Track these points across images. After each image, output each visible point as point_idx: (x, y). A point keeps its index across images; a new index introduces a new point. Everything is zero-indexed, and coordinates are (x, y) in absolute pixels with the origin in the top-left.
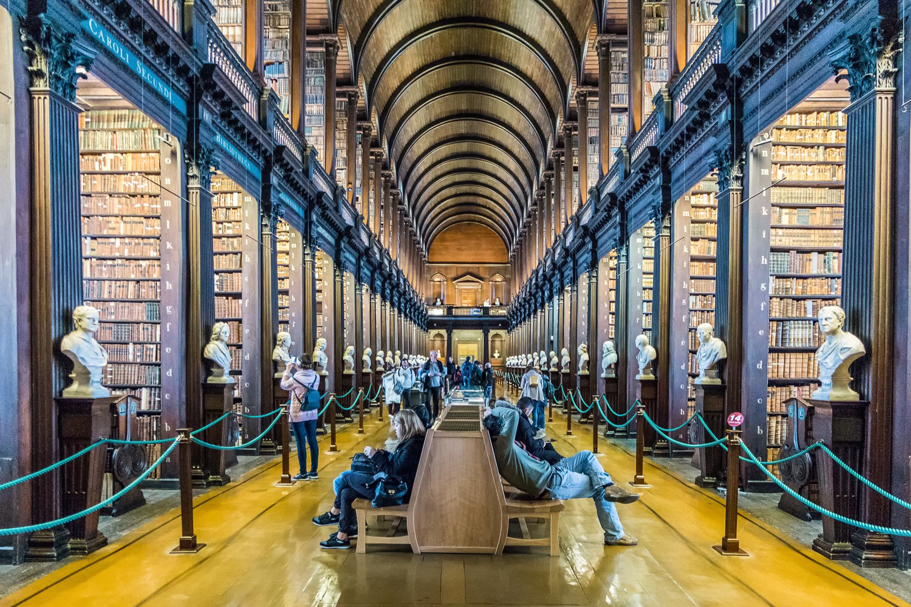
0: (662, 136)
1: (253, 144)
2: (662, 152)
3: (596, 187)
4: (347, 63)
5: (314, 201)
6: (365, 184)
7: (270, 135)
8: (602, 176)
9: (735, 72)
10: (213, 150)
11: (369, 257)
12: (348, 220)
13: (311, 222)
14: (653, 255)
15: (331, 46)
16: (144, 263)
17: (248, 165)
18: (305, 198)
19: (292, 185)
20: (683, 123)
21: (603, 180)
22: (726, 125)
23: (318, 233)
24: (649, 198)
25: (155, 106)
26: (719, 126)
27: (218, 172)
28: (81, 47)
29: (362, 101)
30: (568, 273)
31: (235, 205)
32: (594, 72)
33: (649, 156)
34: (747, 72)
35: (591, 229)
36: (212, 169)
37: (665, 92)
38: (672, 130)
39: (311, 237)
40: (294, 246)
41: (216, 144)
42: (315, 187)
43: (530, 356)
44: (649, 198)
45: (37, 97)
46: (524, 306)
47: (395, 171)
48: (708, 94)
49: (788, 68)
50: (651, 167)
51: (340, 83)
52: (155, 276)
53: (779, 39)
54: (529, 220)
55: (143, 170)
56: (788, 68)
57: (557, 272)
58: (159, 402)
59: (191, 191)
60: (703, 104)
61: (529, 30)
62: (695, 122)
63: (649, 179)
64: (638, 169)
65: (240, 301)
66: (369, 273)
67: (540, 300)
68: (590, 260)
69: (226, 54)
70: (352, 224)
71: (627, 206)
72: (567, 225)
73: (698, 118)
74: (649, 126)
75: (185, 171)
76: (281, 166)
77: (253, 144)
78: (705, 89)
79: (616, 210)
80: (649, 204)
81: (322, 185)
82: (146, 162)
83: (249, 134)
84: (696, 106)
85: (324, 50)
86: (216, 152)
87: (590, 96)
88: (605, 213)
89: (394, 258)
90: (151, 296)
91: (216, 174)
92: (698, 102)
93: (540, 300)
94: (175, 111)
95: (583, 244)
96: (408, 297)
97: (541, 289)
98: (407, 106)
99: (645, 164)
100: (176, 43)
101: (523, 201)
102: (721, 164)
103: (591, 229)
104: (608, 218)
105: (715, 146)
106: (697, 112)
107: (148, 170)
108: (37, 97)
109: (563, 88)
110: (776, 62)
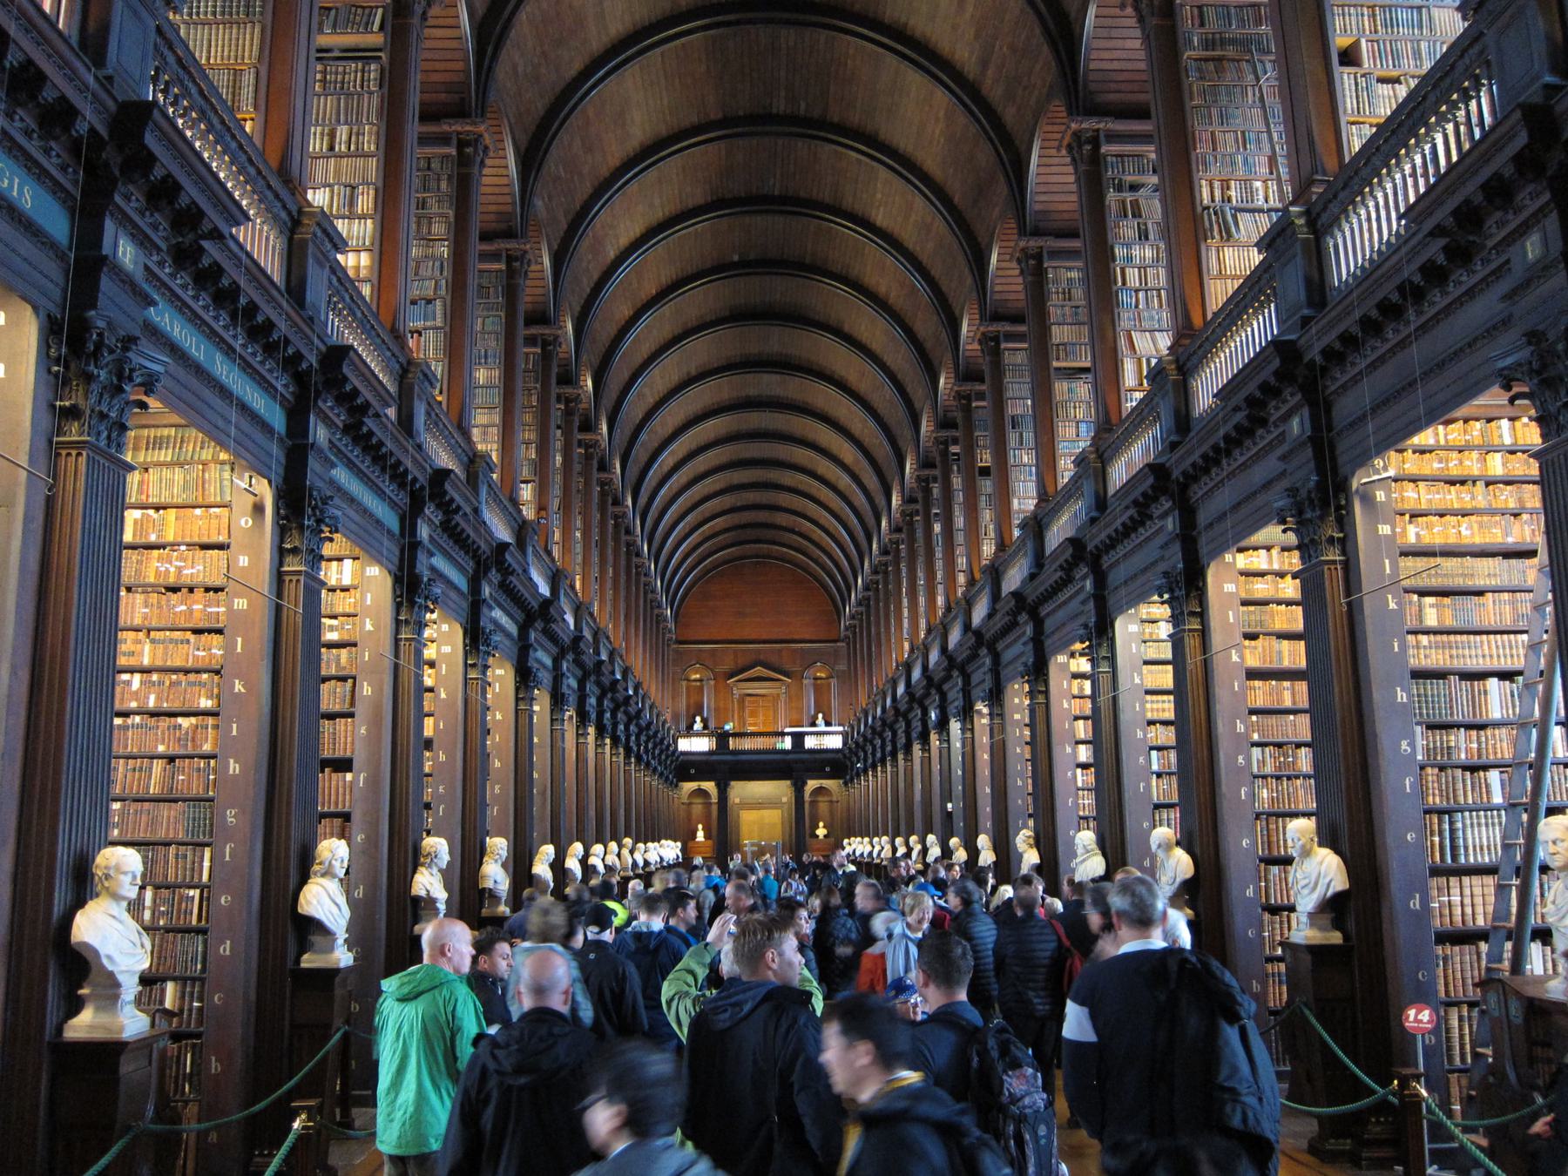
6: (566, 506)
10: (331, 498)
15: (468, 144)
18: (402, 485)
31: (347, 581)
45: (64, 452)
51: (531, 320)
55: (196, 539)
59: (287, 578)
75: (277, 539)
82: (203, 525)
86: (337, 501)
107: (205, 540)
108: (64, 452)
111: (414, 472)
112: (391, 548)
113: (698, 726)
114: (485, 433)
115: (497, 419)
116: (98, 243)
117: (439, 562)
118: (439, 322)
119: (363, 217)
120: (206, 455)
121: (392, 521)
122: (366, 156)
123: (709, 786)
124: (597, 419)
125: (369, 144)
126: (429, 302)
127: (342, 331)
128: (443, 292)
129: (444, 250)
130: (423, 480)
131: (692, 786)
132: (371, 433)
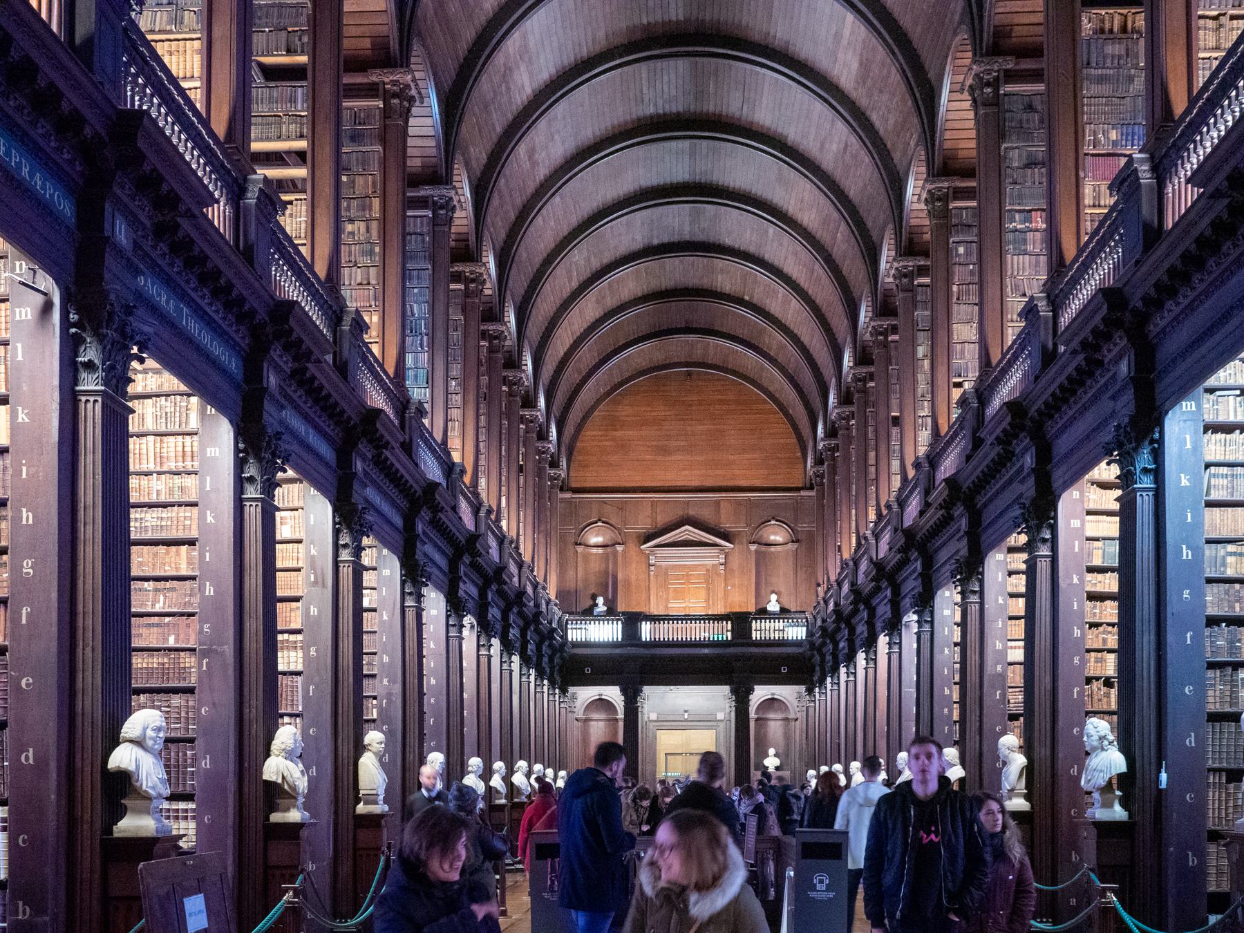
3: (928, 456)
4: (429, 121)
7: (417, 465)
8: (1057, 265)
9: (1136, 303)
11: (475, 554)
14: (1023, 590)
17: (218, 350)
19: (309, 392)
21: (990, 376)
22: (1127, 383)
29: (463, 218)
30: (912, 585)
32: (962, 145)
33: (1009, 418)
37: (1142, 161)
38: (980, 453)
46: (819, 650)
47: (530, 368)
50: (1108, 337)
54: (847, 410)
66: (474, 591)
67: (829, 658)
71: (1051, 428)
72: (905, 479)
74: (1100, 241)
81: (377, 399)
85: (462, 287)
87: (956, 199)
89: (527, 558)
92: (1082, 342)
93: (829, 658)
98: (525, 83)
106: (1082, 356)
109: (871, 255)
116: (260, 378)
117: (370, 492)
124: (548, 427)
127: (291, 290)
130: (355, 419)
132: (313, 378)
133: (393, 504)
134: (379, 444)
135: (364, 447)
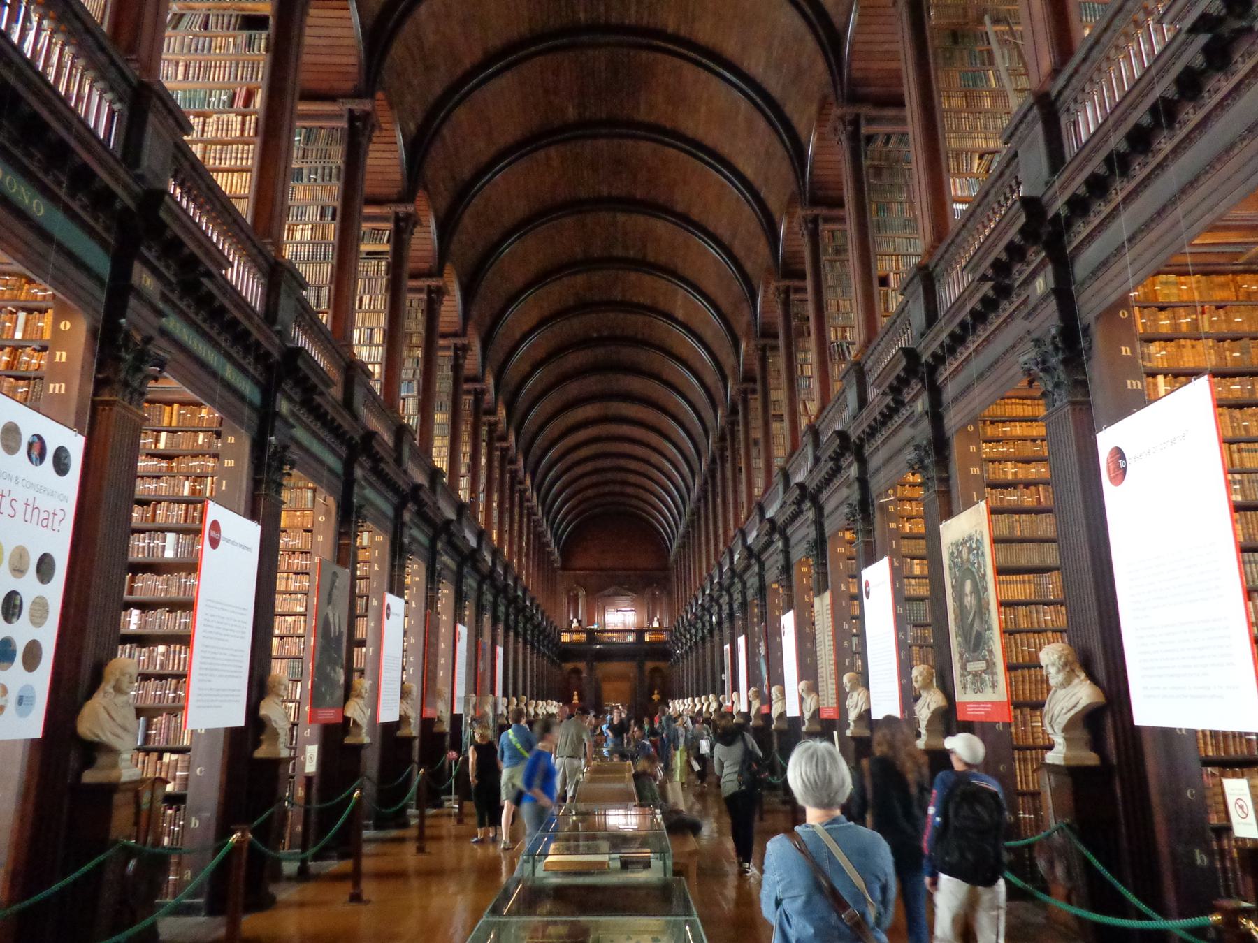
0: (922, 335)
1: (336, 430)
2: (926, 357)
5: (359, 448)
12: (450, 514)
13: (403, 524)
16: (290, 619)
20: (963, 306)
23: (411, 536)
24: (907, 432)
25: (227, 399)
26: (916, 414)
27: (295, 472)
28: (162, 349)
34: (1079, 206)
35: (756, 550)
36: (287, 468)
39: (402, 544)
40: (417, 579)
41: (366, 499)
42: (442, 514)
43: (696, 700)
44: (845, 492)
48: (1011, 248)
49: (975, 367)
52: (301, 631)
53: (1119, 164)
56: (975, 367)
57: (736, 580)
58: (186, 778)
60: (1001, 269)
61: (680, 314)
62: (985, 300)
63: (902, 404)
64: (885, 387)
65: (364, 649)
68: (757, 584)
69: (311, 327)
70: (453, 516)
73: (979, 307)
76: (368, 457)
77: (336, 430)
78: (991, 259)
79: (808, 504)
80: (804, 538)
83: (333, 420)
84: (990, 272)
88: (794, 507)
90: (294, 652)
91: (290, 475)
94: (331, 470)
95: (770, 543)
96: (528, 614)
97: (717, 602)
99: (898, 377)
100: (259, 328)
101: (685, 494)
102: (921, 461)
103: (812, 486)
104: (837, 470)
105: (848, 498)
110: (1014, 307)
111: (404, 487)
112: (389, 525)
113: (575, 624)
114: (439, 452)
115: (447, 442)
118: (415, 393)
119: (377, 345)
120: (301, 484)
121: (390, 512)
122: (379, 312)
123: (582, 665)
125: (380, 305)
126: (410, 382)
128: (418, 376)
129: (419, 353)
131: (569, 666)
133: (386, 498)
134: (376, 459)
135: (362, 459)
